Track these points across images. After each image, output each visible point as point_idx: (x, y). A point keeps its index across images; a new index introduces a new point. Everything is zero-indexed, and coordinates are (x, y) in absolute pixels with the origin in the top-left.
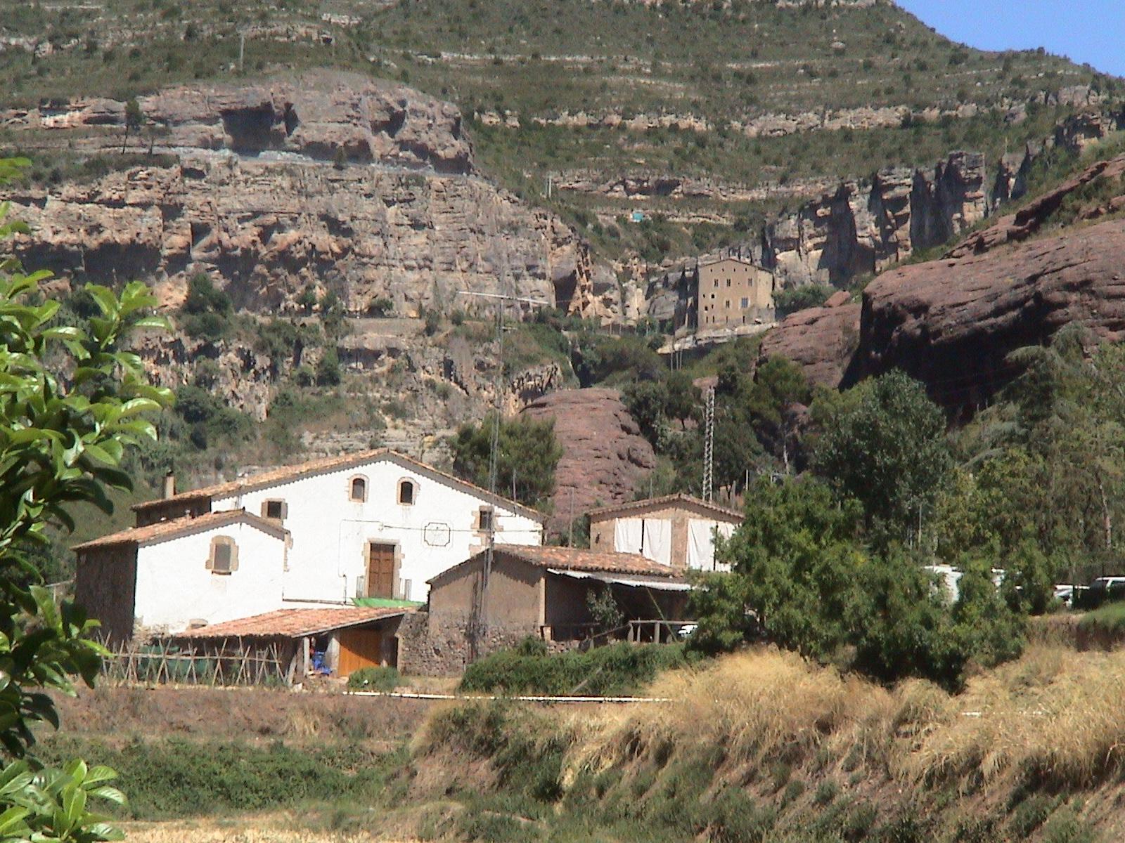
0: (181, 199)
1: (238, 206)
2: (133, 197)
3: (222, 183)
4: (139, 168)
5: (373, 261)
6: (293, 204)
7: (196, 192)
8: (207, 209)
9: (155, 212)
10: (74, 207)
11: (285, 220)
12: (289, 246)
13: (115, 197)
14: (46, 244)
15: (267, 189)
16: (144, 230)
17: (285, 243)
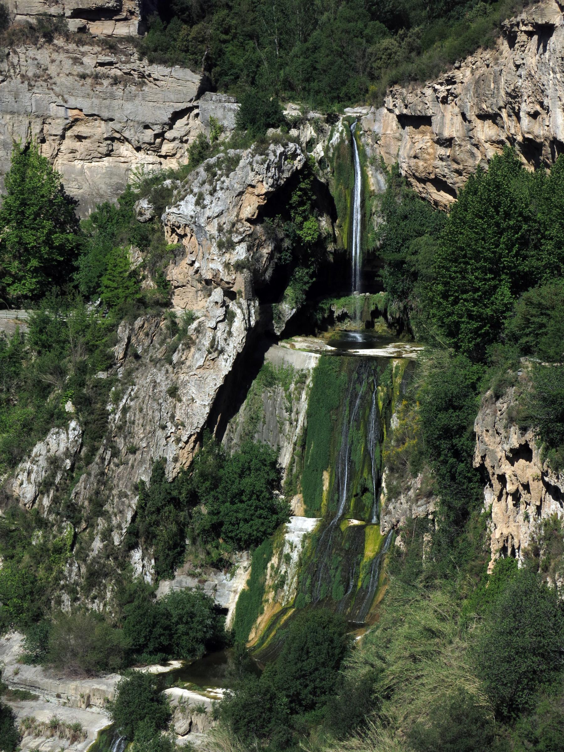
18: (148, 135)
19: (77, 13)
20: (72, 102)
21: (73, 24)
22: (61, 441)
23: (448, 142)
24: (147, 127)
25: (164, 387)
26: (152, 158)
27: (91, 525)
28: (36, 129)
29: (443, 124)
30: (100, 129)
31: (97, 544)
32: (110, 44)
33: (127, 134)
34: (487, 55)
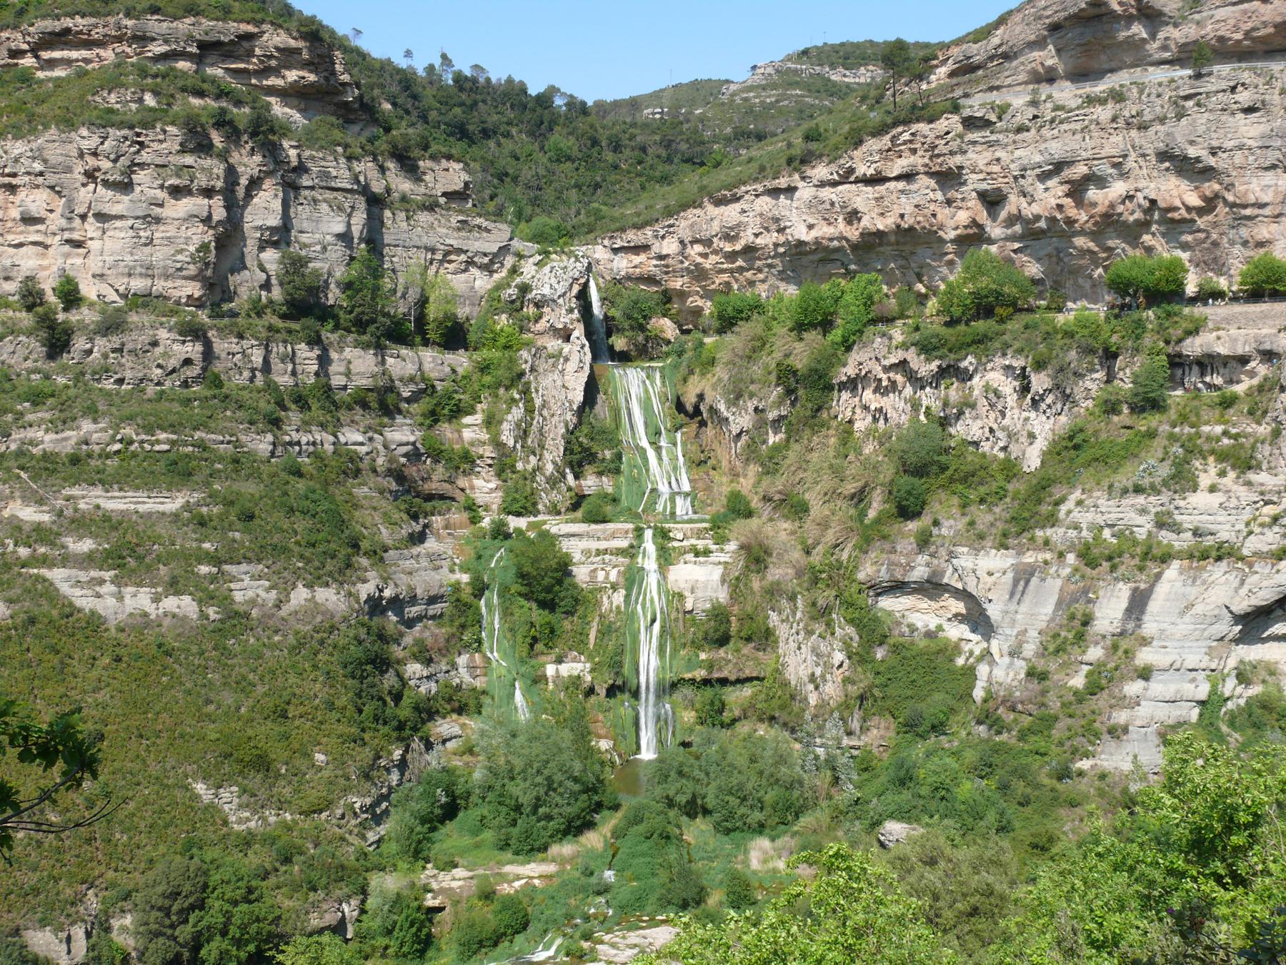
0: (958, 159)
1: (1038, 158)
2: (898, 166)
3: (1021, 129)
4: (900, 129)
5: (1267, 211)
6: (1115, 143)
7: (979, 148)
8: (996, 169)
10: (827, 193)
12: (1112, 206)
13: (871, 171)
14: (801, 243)
15: (1078, 126)
16: (909, 209)
17: (1107, 203)
18: (486, 260)
19: (444, 194)
20: (448, 241)
21: (442, 200)
22: (517, 413)
24: (485, 255)
25: (559, 383)
28: (429, 256)
33: (476, 259)
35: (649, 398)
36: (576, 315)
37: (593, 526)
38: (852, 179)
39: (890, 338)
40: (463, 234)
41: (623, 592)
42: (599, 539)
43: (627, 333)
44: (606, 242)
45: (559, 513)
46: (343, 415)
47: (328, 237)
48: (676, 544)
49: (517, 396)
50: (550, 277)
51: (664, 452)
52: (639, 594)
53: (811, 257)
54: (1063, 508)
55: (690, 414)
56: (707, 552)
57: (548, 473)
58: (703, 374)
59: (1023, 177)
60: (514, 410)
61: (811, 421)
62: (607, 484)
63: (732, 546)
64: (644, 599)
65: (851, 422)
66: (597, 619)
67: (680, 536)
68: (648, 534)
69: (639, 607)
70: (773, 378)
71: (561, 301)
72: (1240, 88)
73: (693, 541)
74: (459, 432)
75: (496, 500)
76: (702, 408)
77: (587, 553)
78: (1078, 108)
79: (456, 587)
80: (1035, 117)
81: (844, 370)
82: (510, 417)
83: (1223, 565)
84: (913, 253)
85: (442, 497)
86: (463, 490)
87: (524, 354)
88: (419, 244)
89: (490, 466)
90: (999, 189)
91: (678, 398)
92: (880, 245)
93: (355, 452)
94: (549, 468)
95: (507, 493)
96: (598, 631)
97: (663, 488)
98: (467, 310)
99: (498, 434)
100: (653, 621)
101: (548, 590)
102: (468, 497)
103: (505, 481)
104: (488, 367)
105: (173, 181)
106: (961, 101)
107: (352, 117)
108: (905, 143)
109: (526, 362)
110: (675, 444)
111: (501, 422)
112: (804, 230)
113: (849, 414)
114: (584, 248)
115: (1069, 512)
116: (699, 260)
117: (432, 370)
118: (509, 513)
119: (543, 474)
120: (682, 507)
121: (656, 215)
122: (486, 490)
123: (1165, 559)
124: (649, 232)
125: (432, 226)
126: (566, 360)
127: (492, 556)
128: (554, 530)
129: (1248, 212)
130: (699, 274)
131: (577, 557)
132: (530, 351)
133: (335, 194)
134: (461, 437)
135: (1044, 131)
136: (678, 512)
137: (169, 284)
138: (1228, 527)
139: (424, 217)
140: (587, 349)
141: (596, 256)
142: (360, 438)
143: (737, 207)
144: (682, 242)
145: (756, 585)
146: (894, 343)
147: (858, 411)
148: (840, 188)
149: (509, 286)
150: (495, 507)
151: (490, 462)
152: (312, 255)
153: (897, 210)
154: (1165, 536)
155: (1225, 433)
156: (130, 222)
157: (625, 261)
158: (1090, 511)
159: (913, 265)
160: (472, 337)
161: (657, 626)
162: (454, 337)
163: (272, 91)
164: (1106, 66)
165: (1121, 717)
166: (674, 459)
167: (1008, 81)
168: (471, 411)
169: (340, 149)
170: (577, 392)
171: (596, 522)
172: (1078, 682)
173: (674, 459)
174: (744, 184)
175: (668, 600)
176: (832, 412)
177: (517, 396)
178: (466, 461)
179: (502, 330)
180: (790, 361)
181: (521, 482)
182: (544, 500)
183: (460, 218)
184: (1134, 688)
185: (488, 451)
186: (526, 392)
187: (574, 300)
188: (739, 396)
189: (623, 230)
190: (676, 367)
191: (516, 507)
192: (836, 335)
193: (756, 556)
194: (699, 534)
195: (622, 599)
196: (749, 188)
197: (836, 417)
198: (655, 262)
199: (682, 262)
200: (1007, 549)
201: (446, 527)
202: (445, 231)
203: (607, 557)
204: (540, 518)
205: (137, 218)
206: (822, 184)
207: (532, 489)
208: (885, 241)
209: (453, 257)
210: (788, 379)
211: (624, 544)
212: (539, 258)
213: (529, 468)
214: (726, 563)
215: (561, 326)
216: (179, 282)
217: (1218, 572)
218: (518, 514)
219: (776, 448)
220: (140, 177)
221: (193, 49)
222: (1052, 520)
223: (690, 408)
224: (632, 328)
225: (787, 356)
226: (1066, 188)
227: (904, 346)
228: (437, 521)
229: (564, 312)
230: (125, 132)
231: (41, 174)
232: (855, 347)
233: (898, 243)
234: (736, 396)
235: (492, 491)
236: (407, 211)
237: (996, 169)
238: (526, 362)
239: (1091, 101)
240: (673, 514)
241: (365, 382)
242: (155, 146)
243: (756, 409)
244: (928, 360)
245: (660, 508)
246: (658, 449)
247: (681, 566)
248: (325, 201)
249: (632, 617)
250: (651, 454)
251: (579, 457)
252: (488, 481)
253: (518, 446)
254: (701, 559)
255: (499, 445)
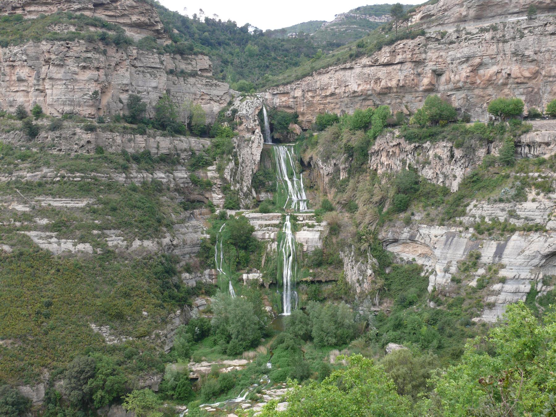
0: (423, 56)
1: (459, 55)
2: (399, 58)
3: (452, 43)
4: (399, 42)
6: (493, 49)
8: (440, 60)
9: (409, 65)
10: (367, 70)
11: (486, 60)
12: (491, 76)
13: (386, 61)
14: (355, 92)
15: (477, 41)
16: (402, 77)
17: (489, 75)
18: (218, 99)
19: (200, 70)
20: (202, 90)
21: (199, 73)
23: (294, 98)
25: (250, 152)
26: (218, 104)
27: (242, 183)
29: (294, 94)
30: (208, 97)
31: (245, 189)
32: (207, 77)
33: (214, 98)
34: (310, 78)
35: (289, 159)
36: (257, 122)
37: (264, 214)
38: (377, 64)
39: (394, 134)
40: (208, 87)
41: (276, 243)
42: (266, 220)
43: (279, 131)
44: (270, 91)
45: (249, 209)
46: (156, 165)
47: (150, 88)
48: (299, 222)
49: (231, 158)
50: (246, 107)
51: (295, 182)
52: (283, 244)
53: (359, 98)
54: (468, 208)
55: (305, 166)
56: (313, 226)
57: (244, 191)
58: (312, 149)
59: (452, 63)
60: (230, 164)
61: (359, 170)
62: (270, 196)
63: (324, 223)
64: (286, 246)
65: (376, 170)
66: (265, 254)
67: (301, 219)
68: (288, 218)
69: (283, 250)
70: (343, 150)
71: (251, 117)
72: (548, 25)
73: (307, 221)
74: (206, 173)
75: (222, 202)
76: (311, 163)
77: (261, 226)
78: (477, 33)
79: (204, 240)
80: (458, 37)
81: (373, 147)
82: (228, 167)
83: (538, 234)
84: (404, 97)
85: (199, 201)
86: (207, 198)
87: (235, 140)
88: (189, 91)
89: (219, 188)
90: (442, 69)
91: (301, 159)
92: (390, 93)
93: (161, 182)
94: (245, 189)
95: (227, 200)
96: (265, 260)
97: (294, 198)
98: (210, 120)
99: (223, 174)
100: (290, 255)
101: (244, 242)
102: (210, 202)
103: (225, 194)
104: (218, 145)
105: (83, 64)
106: (426, 30)
107: (160, 36)
108: (400, 49)
109: (235, 143)
110: (300, 179)
111: (224, 169)
112: (357, 87)
113: (375, 166)
114: (261, 94)
115: (471, 210)
116: (311, 99)
117: (195, 146)
118: (228, 208)
119: (242, 192)
120: (303, 206)
121: (292, 80)
122: (217, 198)
123: (513, 230)
124: (289, 87)
125: (195, 84)
126: (253, 142)
127: (220, 227)
128: (247, 216)
129: (551, 79)
130: (310, 105)
131: (257, 228)
132: (237, 138)
133: (153, 70)
134: (207, 176)
135: (461, 43)
136: (301, 209)
137: (81, 109)
138: (540, 217)
139: (192, 80)
140: (262, 137)
141: (266, 97)
142: (163, 176)
143: (328, 76)
144: (303, 91)
145: (334, 240)
146: (395, 136)
147: (379, 165)
148: (372, 68)
149: (228, 110)
150: (221, 206)
151: (219, 186)
152: (143, 96)
153: (397, 78)
154: (512, 221)
155: (539, 176)
156: (64, 82)
157: (279, 100)
158: (481, 209)
159: (404, 102)
160: (212, 132)
161: (291, 258)
162: (204, 132)
163: (125, 24)
164: (489, 15)
165: (492, 299)
166: (299, 185)
167: (446, 22)
168: (211, 164)
169: (155, 50)
170: (257, 156)
171: (265, 212)
172: (474, 283)
173: (299, 185)
174: (331, 66)
175: (296, 247)
176: (368, 166)
177: (231, 158)
178: (208, 186)
179: (225, 129)
180: (349, 144)
181: (233, 195)
182: (243, 202)
183: (207, 80)
184: (497, 287)
185: (218, 182)
186: (235, 155)
187: (256, 116)
188: (328, 158)
189: (278, 86)
190: (300, 146)
191: (231, 206)
192: (370, 133)
193: (335, 228)
194: (310, 218)
195: (276, 246)
196: (332, 68)
197: (370, 168)
198: (292, 100)
199: (303, 100)
200: (444, 225)
201: (200, 214)
202: (200, 86)
203: (270, 228)
204: (241, 210)
205: (67, 80)
206: (365, 66)
207: (238, 198)
208: (392, 91)
209: (204, 97)
210: (350, 151)
211: (277, 222)
212: (241, 98)
213: (236, 189)
214: (321, 231)
215: (250, 127)
216: (85, 108)
217: (534, 236)
218: (232, 209)
219: (344, 181)
220: (69, 62)
221: (91, 6)
222: (463, 213)
223: (306, 163)
224: (281, 128)
225: (348, 141)
226: (470, 68)
227: (399, 137)
228: (197, 211)
229: (252, 121)
230: (62, 42)
231: (26, 61)
232: (378, 138)
233: (397, 92)
234: (326, 158)
235: (220, 199)
236: (184, 77)
237: (440, 60)
238: (235, 143)
239: (483, 30)
240: (299, 209)
241: (165, 151)
242: (75, 48)
243: (335, 164)
244: (410, 143)
245: (293, 207)
246: (292, 181)
247: (302, 232)
248: (148, 72)
249: (280, 254)
250: (289, 183)
251: (258, 183)
252: (218, 195)
253: (232, 180)
254: (311, 229)
255: (224, 179)
